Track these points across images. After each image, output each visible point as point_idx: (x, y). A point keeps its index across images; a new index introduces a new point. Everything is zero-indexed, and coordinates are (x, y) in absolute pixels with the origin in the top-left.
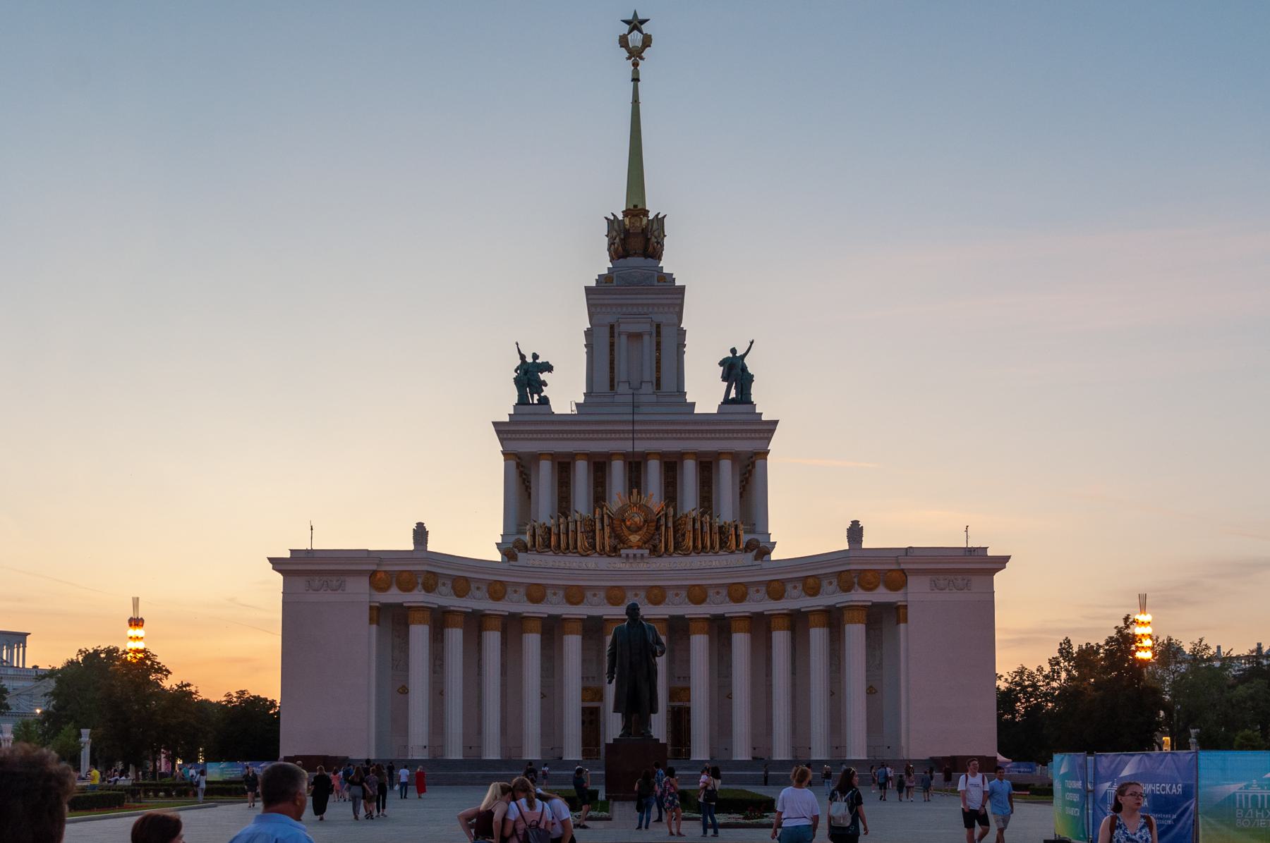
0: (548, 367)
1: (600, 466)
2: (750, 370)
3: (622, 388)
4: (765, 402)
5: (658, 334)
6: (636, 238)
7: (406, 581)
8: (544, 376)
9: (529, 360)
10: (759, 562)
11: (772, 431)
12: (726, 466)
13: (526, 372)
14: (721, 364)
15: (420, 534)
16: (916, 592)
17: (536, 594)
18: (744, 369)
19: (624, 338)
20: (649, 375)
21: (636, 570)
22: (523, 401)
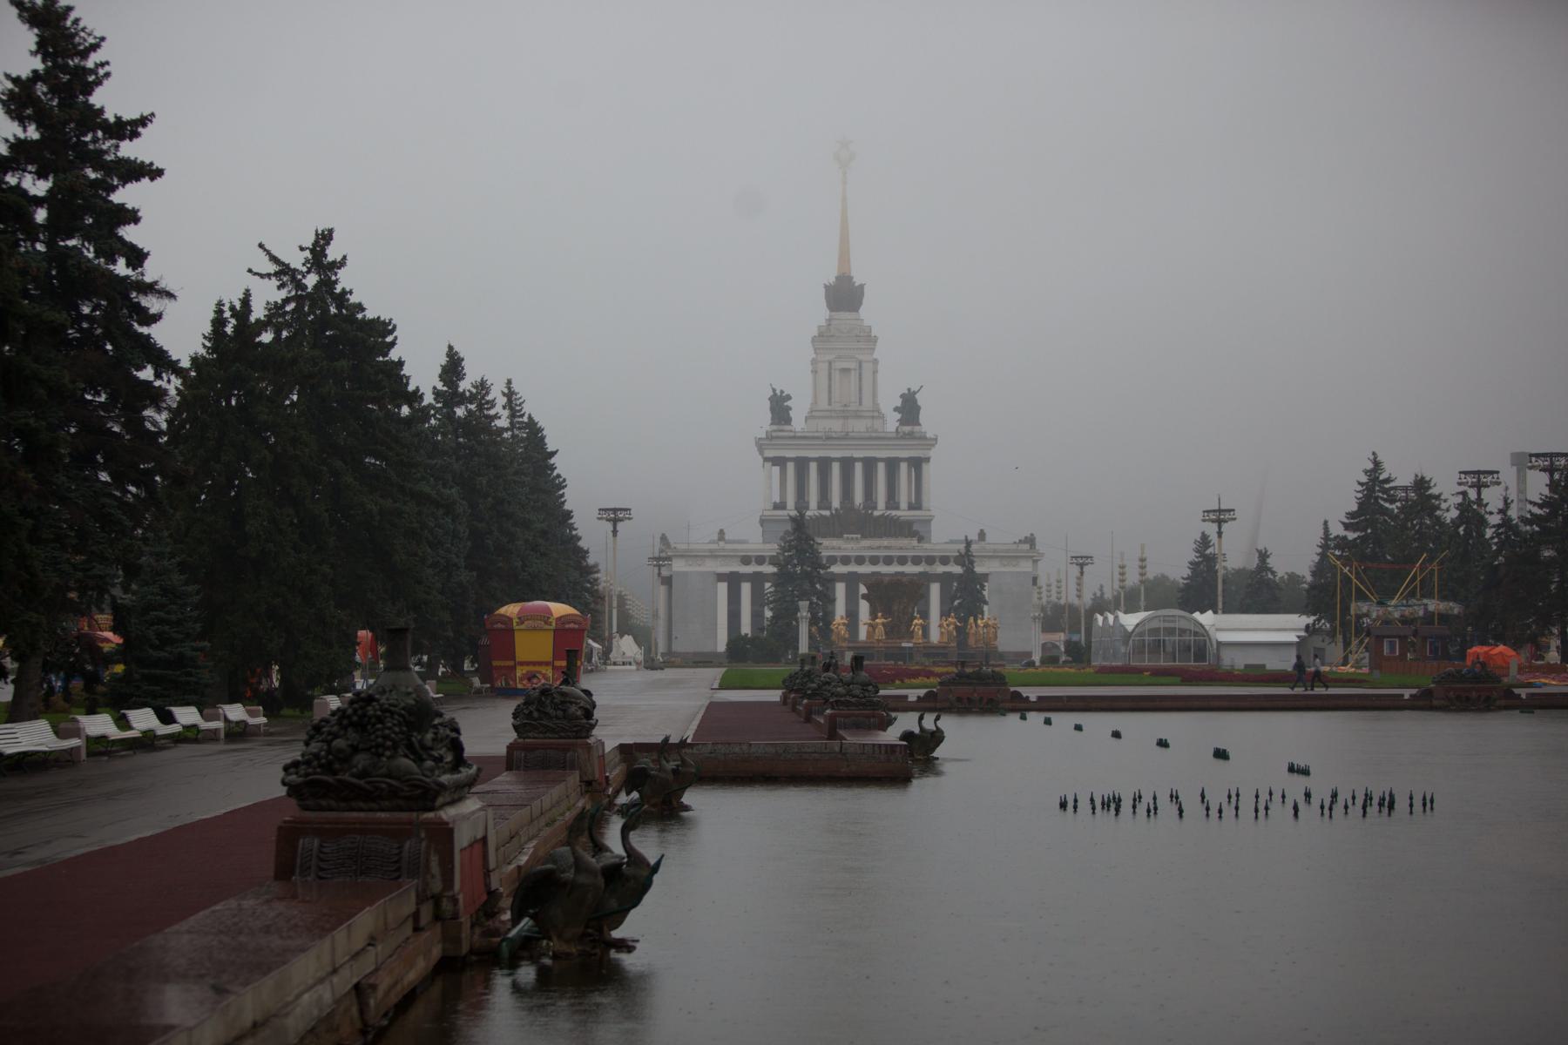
0: (789, 398)
4: (928, 422)
6: (844, 295)
12: (904, 467)
14: (902, 396)
18: (915, 401)
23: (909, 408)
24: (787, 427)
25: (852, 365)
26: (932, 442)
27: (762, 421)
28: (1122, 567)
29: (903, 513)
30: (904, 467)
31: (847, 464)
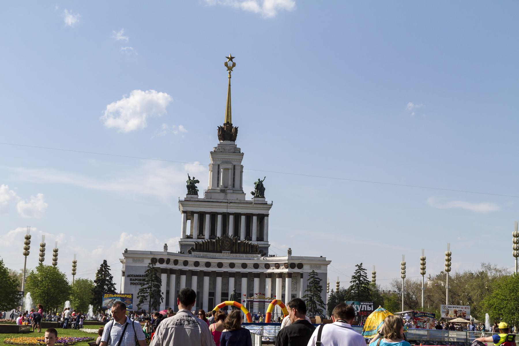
0: (198, 182)
2: (264, 186)
4: (268, 197)
7: (161, 261)
8: (196, 185)
9: (192, 179)
10: (262, 257)
11: (270, 208)
12: (255, 219)
14: (255, 183)
15: (166, 247)
16: (307, 269)
17: (197, 264)
18: (262, 185)
20: (230, 182)
21: (226, 258)
23: (260, 189)
24: (195, 196)
26: (269, 206)
27: (183, 194)
28: (374, 274)
29: (254, 242)
30: (255, 219)
31: (225, 216)
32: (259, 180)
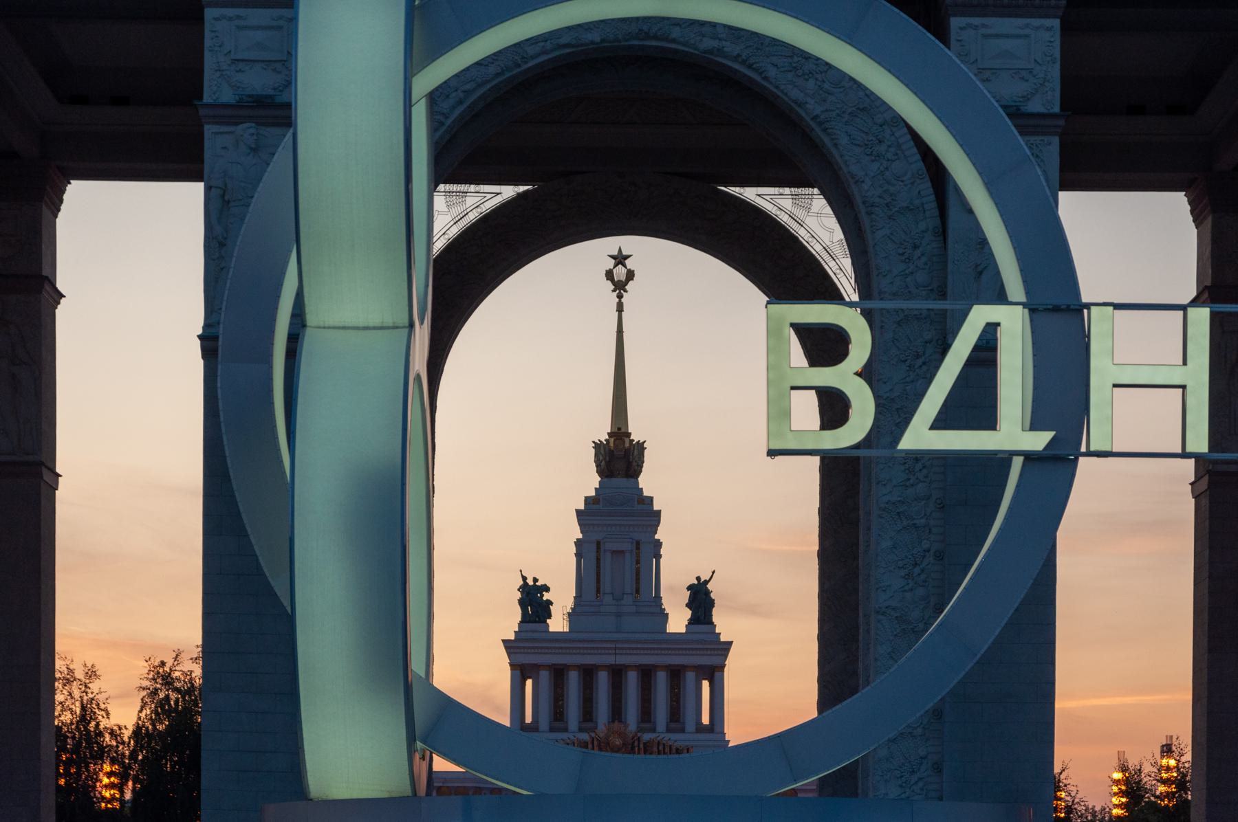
0: (546, 589)
1: (588, 673)
3: (608, 599)
5: (638, 548)
9: (530, 582)
11: (728, 650)
12: (690, 676)
13: (528, 594)
14: (689, 588)
18: (708, 593)
19: (608, 555)
22: (525, 619)
23: (701, 599)
25: (626, 546)
31: (617, 673)
32: (698, 578)
